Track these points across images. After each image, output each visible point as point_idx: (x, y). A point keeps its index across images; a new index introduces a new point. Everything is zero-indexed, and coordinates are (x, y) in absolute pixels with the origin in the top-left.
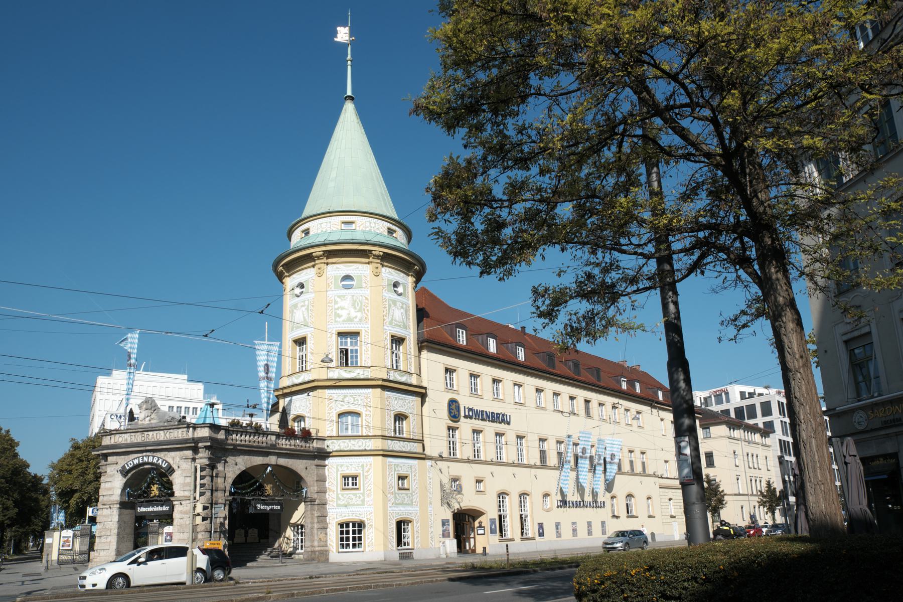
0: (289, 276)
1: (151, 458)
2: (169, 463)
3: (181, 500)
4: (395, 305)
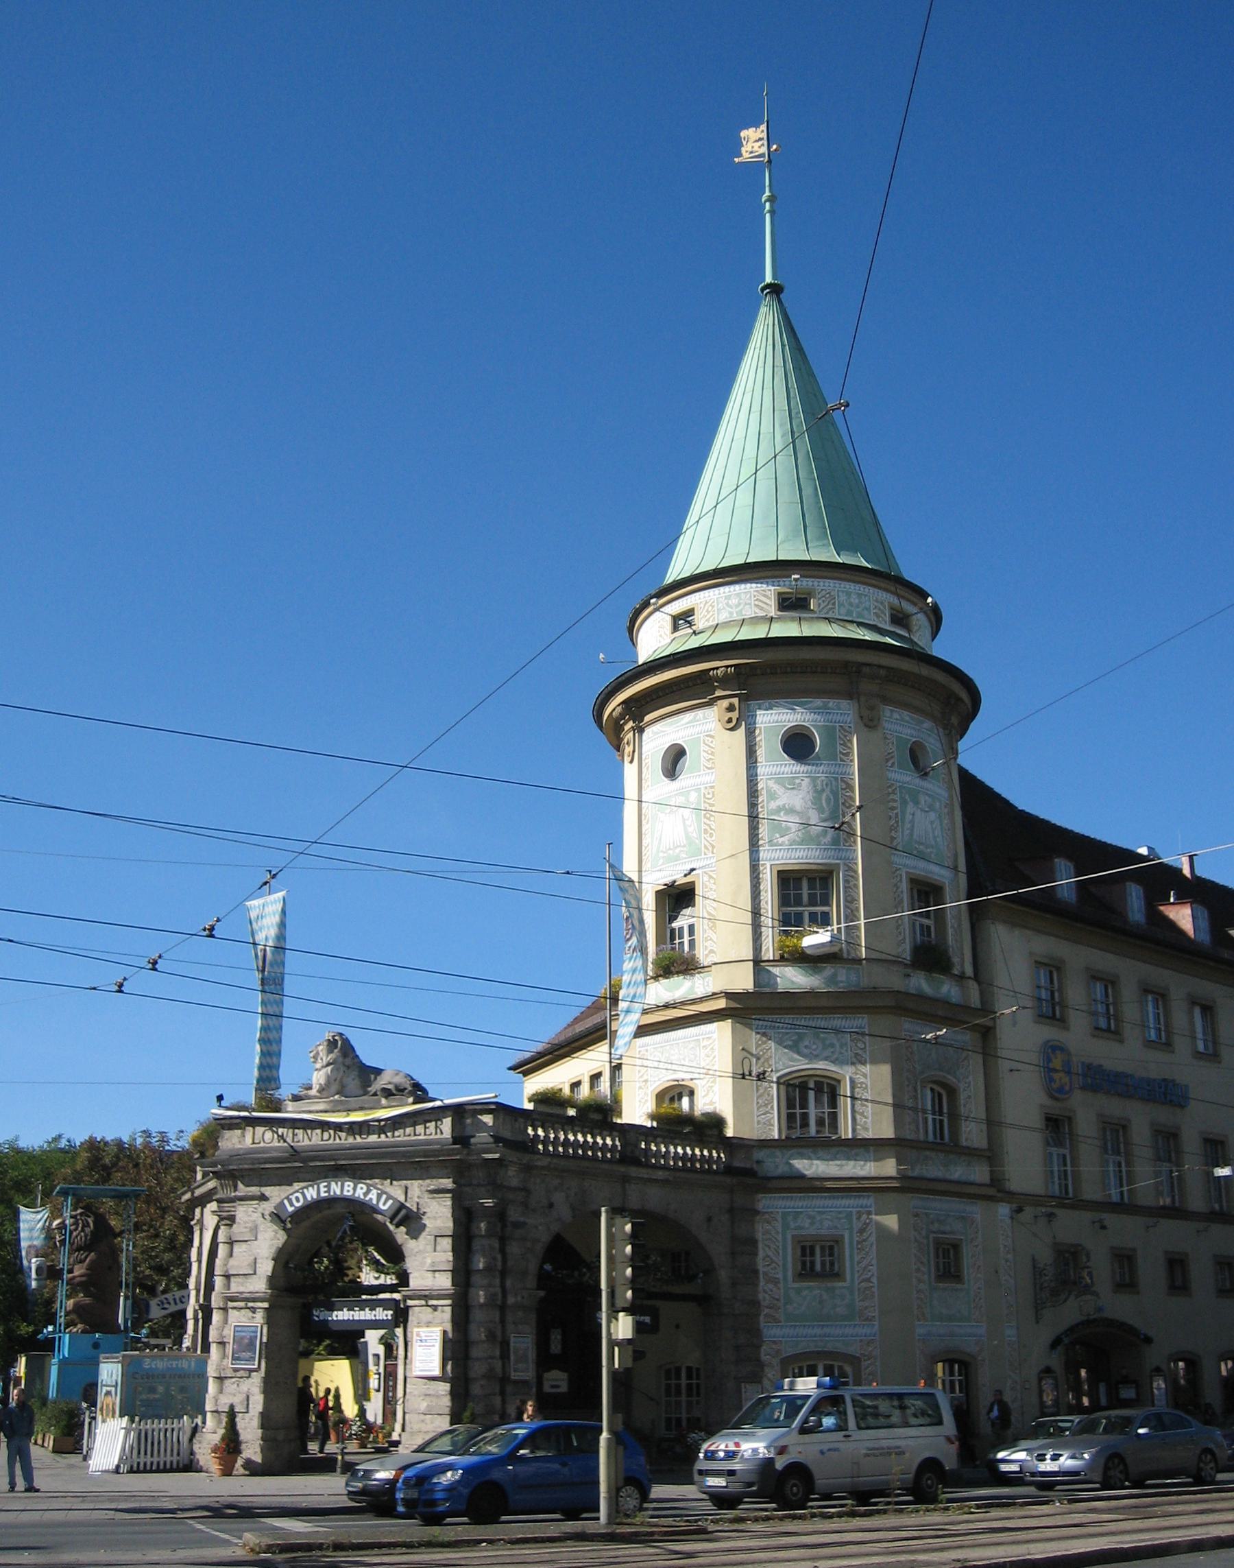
2: (395, 1200)
3: (426, 1296)
4: (917, 803)
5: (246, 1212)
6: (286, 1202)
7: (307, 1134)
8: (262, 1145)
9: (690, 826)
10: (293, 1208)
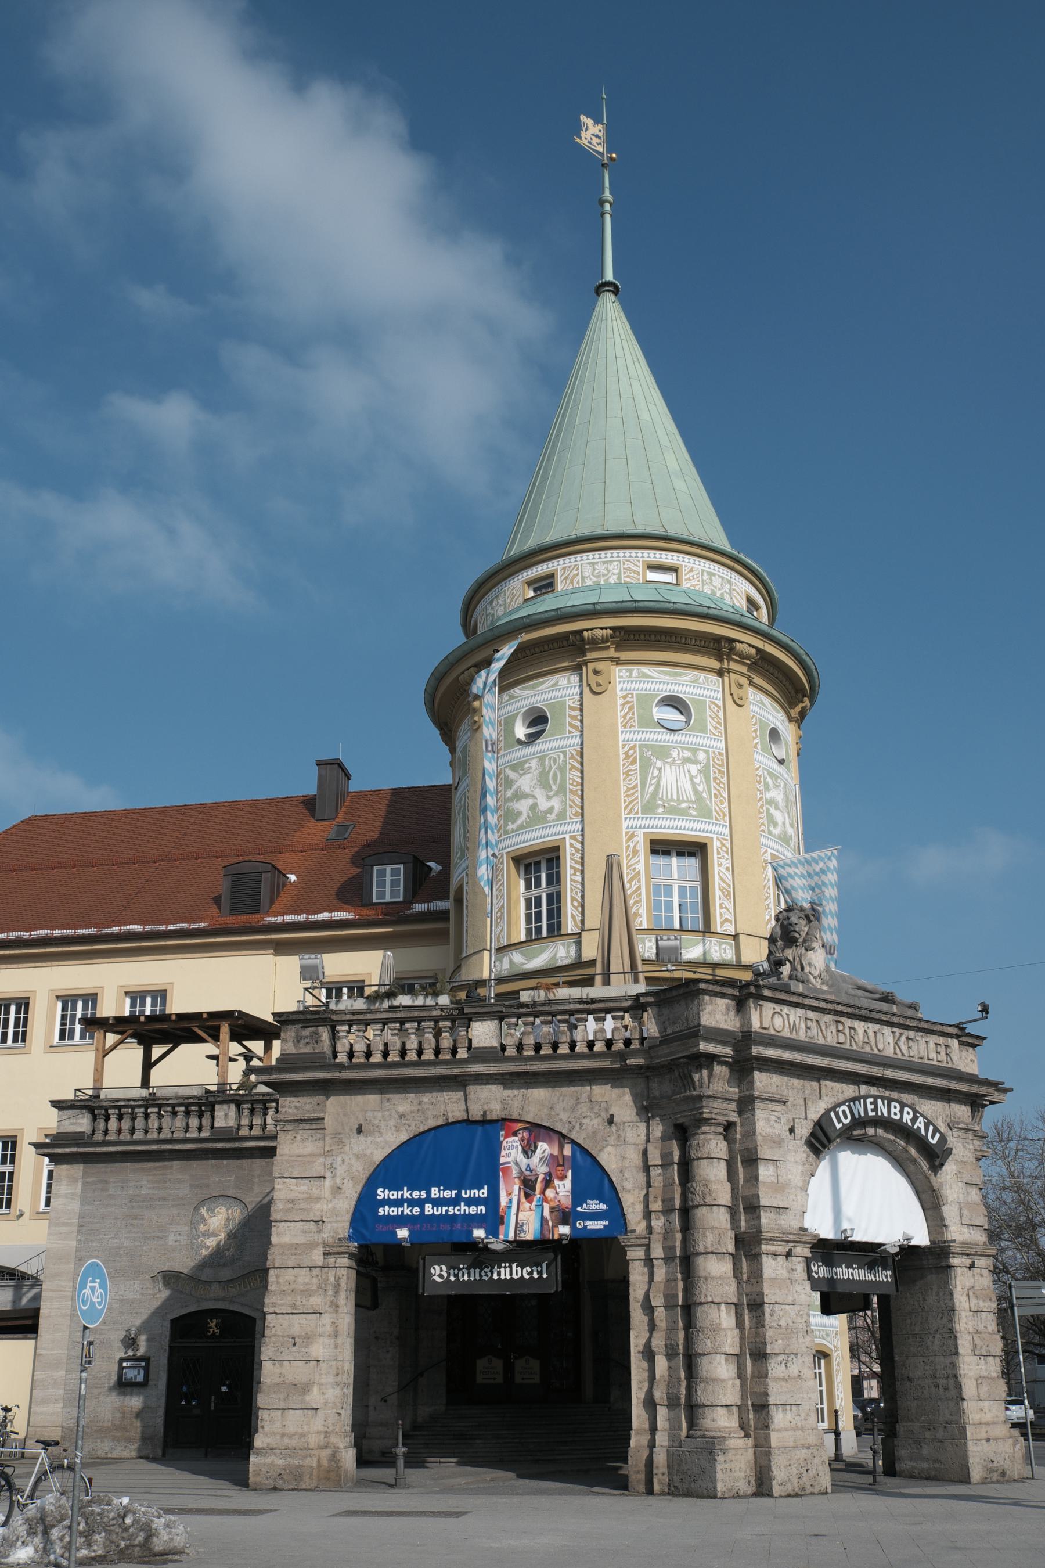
0: (619, 662)
1: (895, 1108)
5: (768, 1120)
6: (832, 1114)
7: (821, 1030)
8: (772, 1032)
9: (699, 785)
10: (841, 1125)
